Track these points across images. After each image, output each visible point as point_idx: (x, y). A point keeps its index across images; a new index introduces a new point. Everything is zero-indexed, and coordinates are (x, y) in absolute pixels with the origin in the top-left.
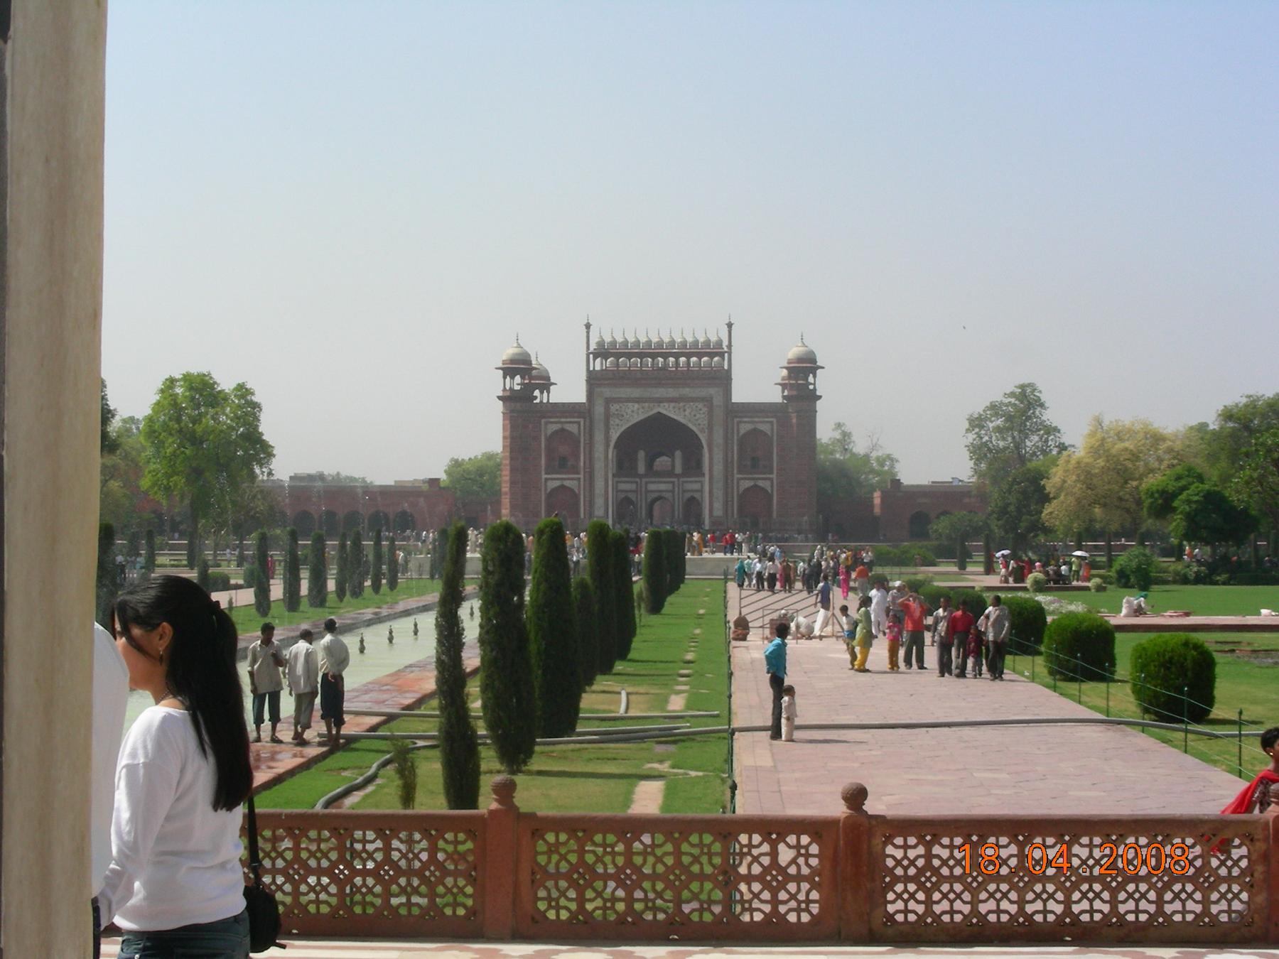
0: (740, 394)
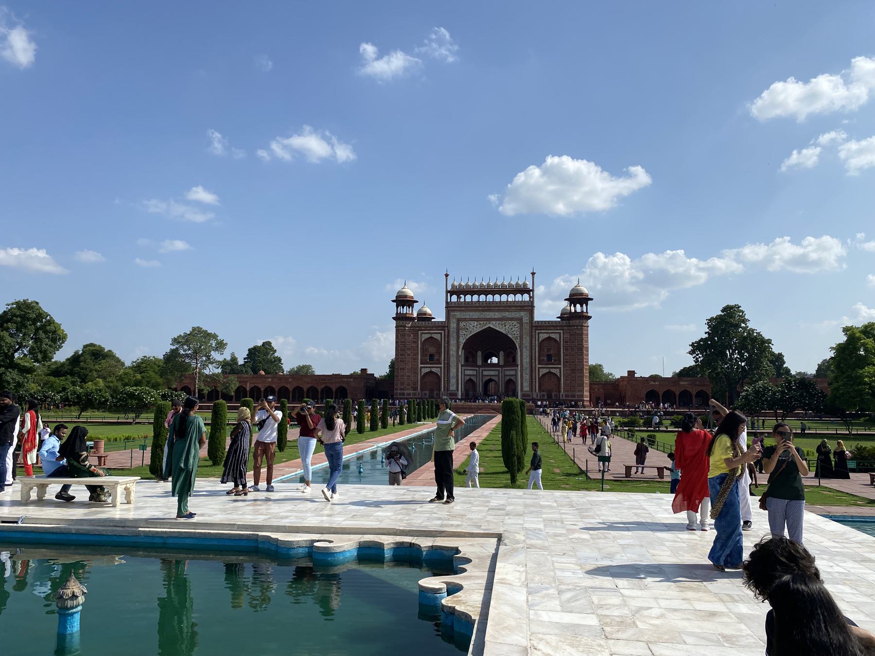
0: (538, 317)
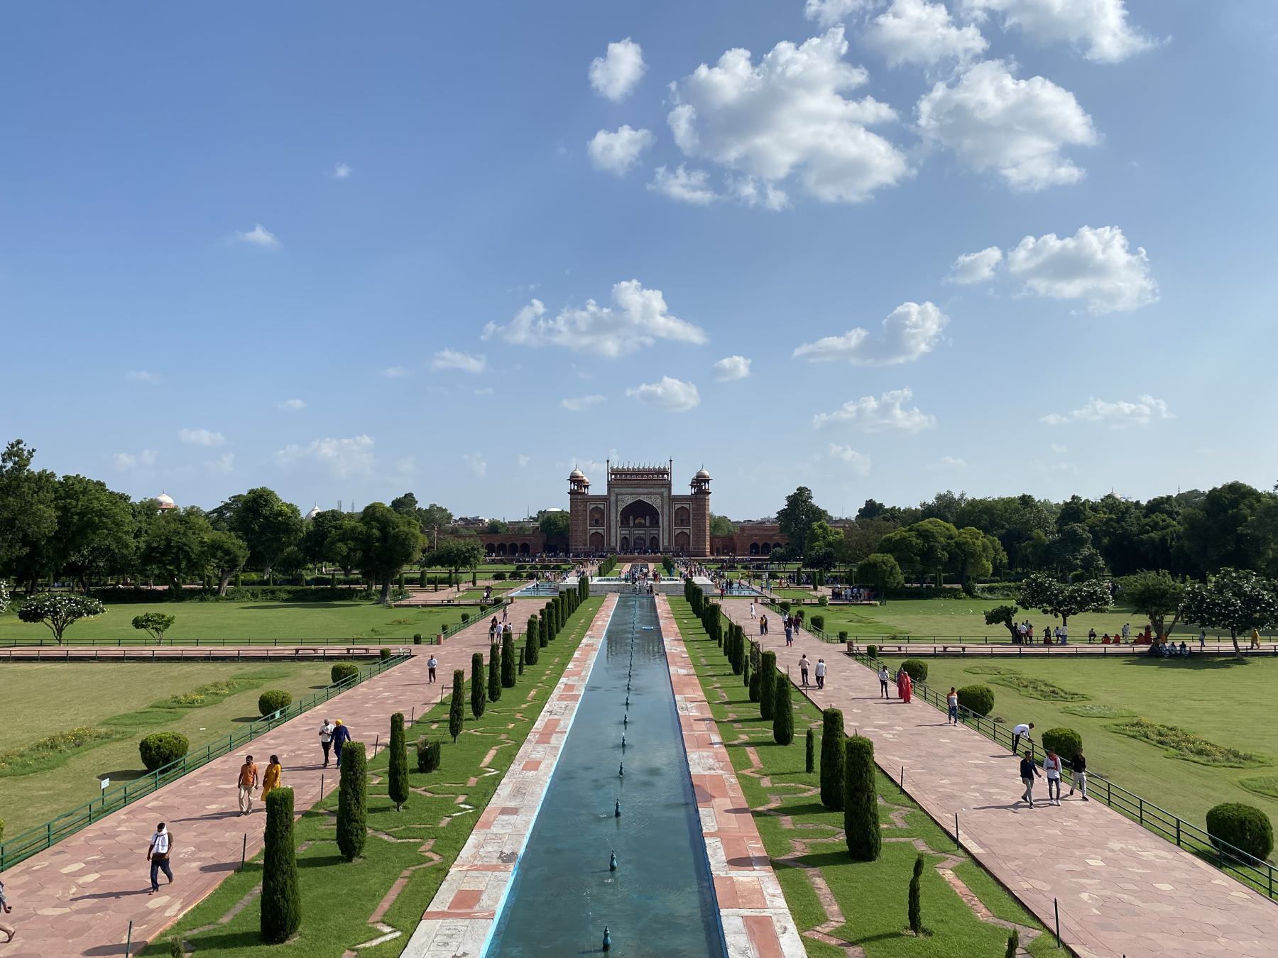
0: (675, 491)
